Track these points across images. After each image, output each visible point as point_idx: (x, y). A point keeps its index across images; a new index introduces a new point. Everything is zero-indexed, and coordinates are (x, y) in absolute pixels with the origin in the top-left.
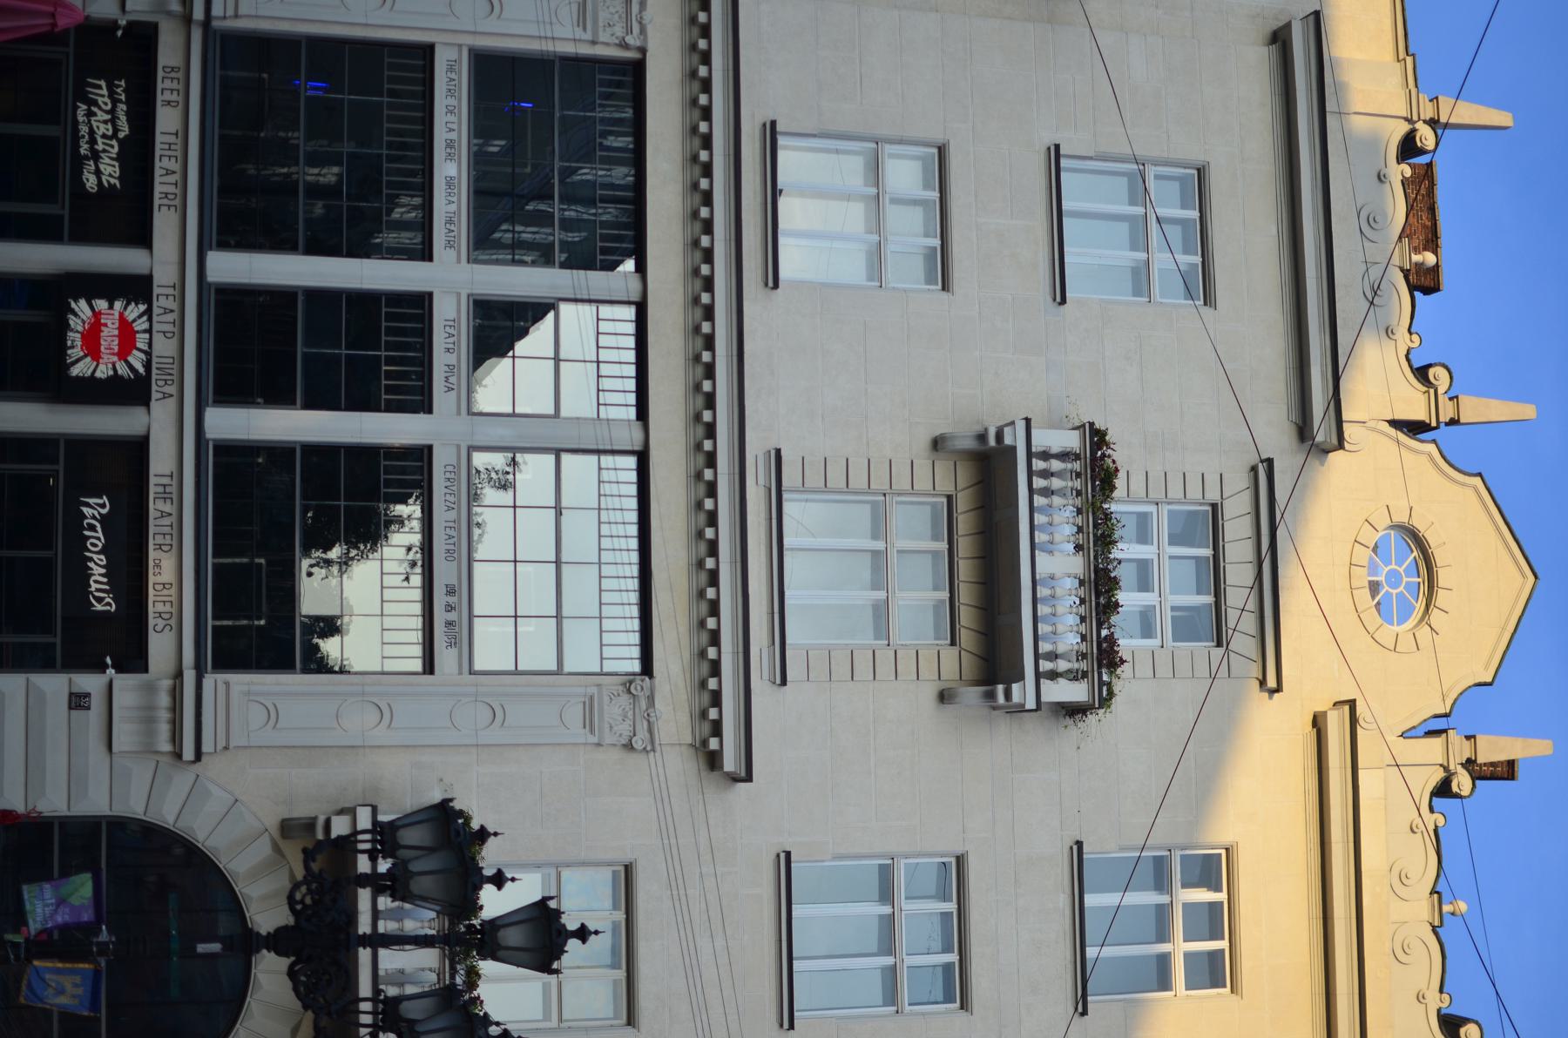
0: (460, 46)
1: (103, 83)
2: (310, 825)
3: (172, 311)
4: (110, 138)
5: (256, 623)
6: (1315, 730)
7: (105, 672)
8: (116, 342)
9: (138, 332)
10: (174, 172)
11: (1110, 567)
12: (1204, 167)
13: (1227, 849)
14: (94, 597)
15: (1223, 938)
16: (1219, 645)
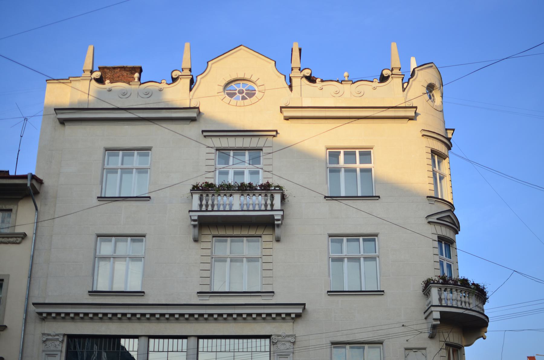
6: (289, 120)
11: (237, 186)
12: (105, 149)
13: (327, 149)
15: (355, 151)
16: (262, 150)
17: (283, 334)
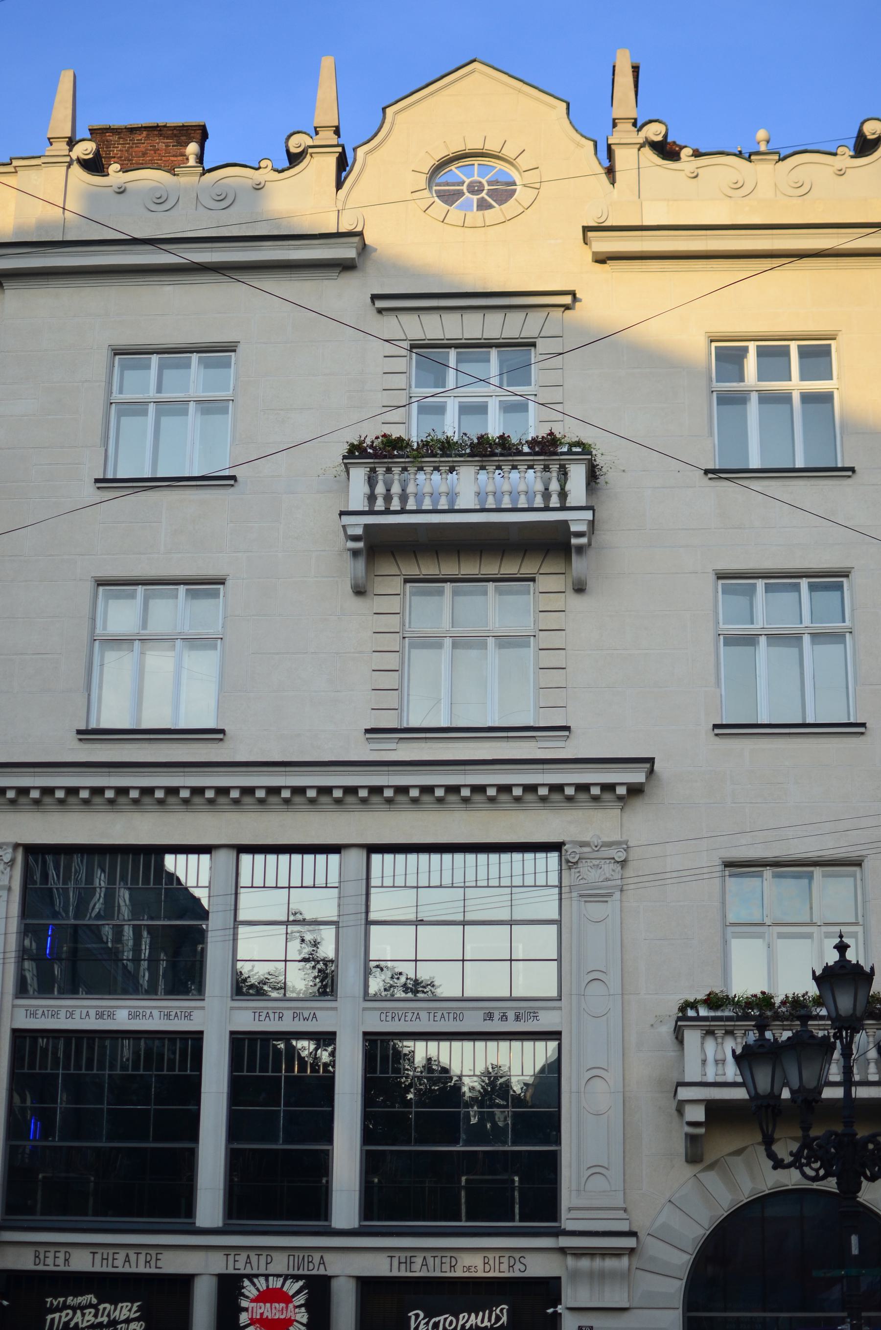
0: (13, 1006)
1: (49, 1317)
2: (692, 1139)
3: (248, 1257)
4: (97, 1310)
5: (517, 1184)
6: (608, 262)
7: (560, 1314)
8: (277, 1305)
9: (268, 1287)
10: (127, 1255)
11: (469, 443)
13: (712, 341)
14: (496, 1323)
15: (788, 346)
16: (534, 345)
17: (595, 841)
